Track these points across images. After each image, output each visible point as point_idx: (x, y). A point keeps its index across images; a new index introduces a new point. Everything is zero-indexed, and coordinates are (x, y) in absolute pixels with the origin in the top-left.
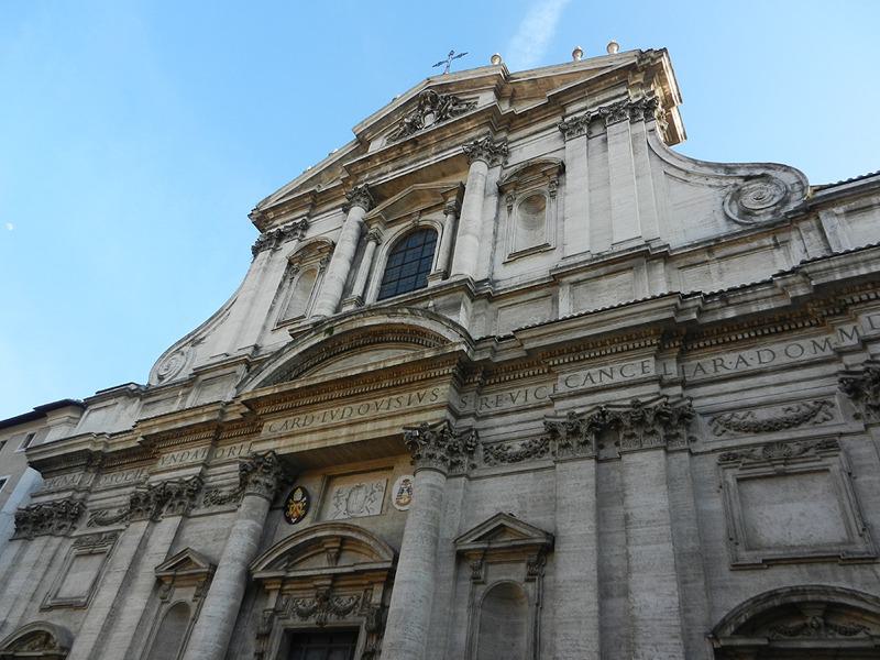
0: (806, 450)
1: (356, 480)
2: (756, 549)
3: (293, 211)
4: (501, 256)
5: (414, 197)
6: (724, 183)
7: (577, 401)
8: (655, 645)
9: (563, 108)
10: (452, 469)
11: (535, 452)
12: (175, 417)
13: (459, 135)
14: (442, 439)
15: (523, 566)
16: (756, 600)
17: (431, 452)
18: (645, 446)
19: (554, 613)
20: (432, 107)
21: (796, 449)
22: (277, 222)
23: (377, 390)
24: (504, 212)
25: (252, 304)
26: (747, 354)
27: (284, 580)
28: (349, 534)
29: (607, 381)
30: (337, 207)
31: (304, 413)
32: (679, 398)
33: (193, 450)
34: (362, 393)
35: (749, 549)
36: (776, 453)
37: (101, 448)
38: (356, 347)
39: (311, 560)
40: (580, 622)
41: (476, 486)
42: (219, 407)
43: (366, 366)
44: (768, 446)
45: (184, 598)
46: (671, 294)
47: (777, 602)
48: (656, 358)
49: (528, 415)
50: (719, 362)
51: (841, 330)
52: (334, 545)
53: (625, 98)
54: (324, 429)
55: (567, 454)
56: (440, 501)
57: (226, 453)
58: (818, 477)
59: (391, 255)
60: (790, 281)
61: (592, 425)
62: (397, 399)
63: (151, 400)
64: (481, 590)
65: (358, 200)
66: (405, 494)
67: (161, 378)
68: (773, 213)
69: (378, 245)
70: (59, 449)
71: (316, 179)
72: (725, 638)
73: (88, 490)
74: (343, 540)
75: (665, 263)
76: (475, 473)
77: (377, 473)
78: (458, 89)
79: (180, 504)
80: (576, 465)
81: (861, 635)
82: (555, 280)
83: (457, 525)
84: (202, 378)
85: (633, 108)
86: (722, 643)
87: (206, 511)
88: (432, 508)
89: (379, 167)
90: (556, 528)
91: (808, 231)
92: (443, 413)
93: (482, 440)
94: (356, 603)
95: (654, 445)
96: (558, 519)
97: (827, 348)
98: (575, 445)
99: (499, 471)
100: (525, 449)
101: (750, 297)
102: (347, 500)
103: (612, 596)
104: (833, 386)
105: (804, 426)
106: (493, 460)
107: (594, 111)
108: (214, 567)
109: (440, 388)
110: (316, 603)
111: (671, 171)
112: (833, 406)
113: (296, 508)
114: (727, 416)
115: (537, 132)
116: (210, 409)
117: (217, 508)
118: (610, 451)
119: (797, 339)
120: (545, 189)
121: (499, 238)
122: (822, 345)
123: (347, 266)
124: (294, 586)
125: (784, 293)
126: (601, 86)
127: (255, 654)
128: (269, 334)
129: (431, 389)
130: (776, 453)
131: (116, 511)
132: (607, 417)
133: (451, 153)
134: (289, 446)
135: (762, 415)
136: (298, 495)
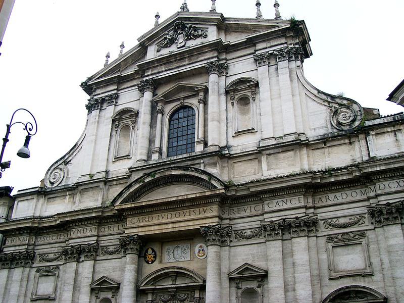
0: (355, 236)
2: (338, 272)
3: (107, 85)
4: (231, 133)
5: (182, 89)
7: (273, 215)
9: (255, 45)
10: (222, 244)
11: (256, 235)
14: (218, 232)
17: (214, 238)
18: (300, 235)
19: (269, 298)
21: (352, 235)
22: (98, 91)
24: (230, 105)
25: (95, 143)
26: (338, 194)
28: (181, 271)
29: (285, 206)
30: (133, 86)
32: (313, 215)
35: (335, 272)
36: (346, 237)
37: (36, 225)
39: (163, 280)
41: (233, 249)
42: (102, 210)
44: (343, 234)
47: (342, 291)
48: (304, 196)
49: (253, 219)
50: (327, 197)
51: (370, 188)
56: (219, 257)
59: (170, 120)
60: (354, 169)
63: (51, 196)
64: (240, 291)
66: (201, 252)
67: (52, 183)
68: (350, 125)
69: (163, 115)
70: (14, 225)
71: (118, 67)
75: (307, 148)
76: (232, 244)
79: (92, 255)
82: (259, 153)
83: (228, 266)
84: (80, 188)
85: (288, 53)
88: (217, 261)
89: (157, 66)
90: (268, 267)
92: (216, 220)
93: (233, 229)
96: (269, 264)
97: (365, 194)
98: (273, 234)
101: (340, 174)
107: (271, 50)
109: (213, 207)
111: (308, 93)
112: (365, 218)
113: (150, 257)
114: (330, 221)
115: (241, 57)
116: (96, 210)
117: (110, 257)
118: (287, 236)
119: (355, 189)
120: (249, 94)
121: (228, 121)
123: (147, 128)
125: (351, 173)
126: (273, 36)
129: (209, 207)
130: (346, 237)
133: (198, 65)
136: (150, 251)
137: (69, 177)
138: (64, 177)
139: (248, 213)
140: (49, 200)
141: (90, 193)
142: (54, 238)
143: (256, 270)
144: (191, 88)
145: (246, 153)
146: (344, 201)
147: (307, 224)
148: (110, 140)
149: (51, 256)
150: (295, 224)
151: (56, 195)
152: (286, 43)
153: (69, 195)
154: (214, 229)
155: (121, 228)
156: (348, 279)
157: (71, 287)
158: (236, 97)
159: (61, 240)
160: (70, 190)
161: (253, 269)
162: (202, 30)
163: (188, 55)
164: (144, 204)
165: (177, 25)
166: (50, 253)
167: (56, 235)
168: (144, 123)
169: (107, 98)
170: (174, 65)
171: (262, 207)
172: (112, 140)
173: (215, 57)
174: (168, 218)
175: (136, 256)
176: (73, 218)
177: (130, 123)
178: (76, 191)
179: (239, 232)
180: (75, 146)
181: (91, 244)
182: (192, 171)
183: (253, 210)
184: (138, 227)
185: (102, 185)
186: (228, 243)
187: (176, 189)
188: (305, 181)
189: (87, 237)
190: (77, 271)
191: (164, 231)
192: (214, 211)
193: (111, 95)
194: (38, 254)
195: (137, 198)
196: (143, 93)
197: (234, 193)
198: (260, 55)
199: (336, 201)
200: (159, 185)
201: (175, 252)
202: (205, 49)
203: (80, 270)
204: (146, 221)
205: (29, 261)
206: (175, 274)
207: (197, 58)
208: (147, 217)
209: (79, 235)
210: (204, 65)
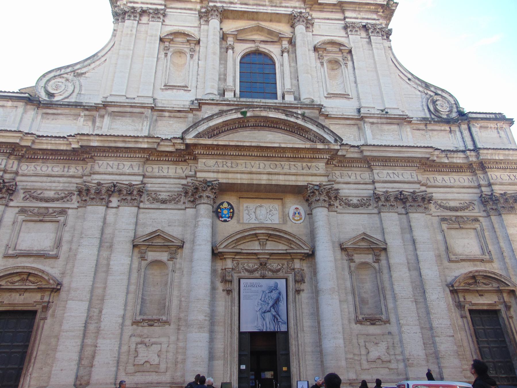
1: (258, 202)
5: (260, 29)
6: (426, 91)
7: (386, 185)
8: (433, 289)
9: (343, 12)
11: (365, 205)
12: (116, 139)
15: (371, 256)
16: (466, 274)
17: (324, 198)
23: (283, 157)
26: (446, 178)
27: (238, 253)
29: (397, 179)
33: (127, 164)
34: (273, 157)
35: (453, 255)
36: (460, 220)
37: (29, 144)
38: (258, 126)
40: (403, 280)
42: (159, 141)
43: (280, 143)
44: (457, 217)
45: (159, 258)
46: (431, 147)
52: (264, 238)
53: (378, 22)
54: (251, 173)
55: (383, 209)
57: (156, 170)
58: (472, 230)
59: (240, 63)
61: (396, 198)
62: (294, 165)
65: (217, 15)
66: (297, 215)
68: (447, 115)
72: (457, 287)
73: (17, 173)
74: (270, 235)
77: (270, 200)
80: (390, 214)
81: (490, 285)
84: (110, 109)
85: (381, 29)
86: (455, 288)
87: (153, 206)
91: (465, 130)
94: (282, 267)
95: (421, 211)
97: (473, 182)
99: (349, 212)
100: (359, 203)
102: (255, 212)
103: (411, 270)
104: (476, 197)
105: (466, 211)
106: (344, 206)
107: (364, 22)
108: (184, 243)
110: (256, 266)
111: (401, 75)
112: (475, 205)
115: (328, 19)
116: (150, 140)
117: (163, 206)
120: (340, 59)
122: (471, 180)
124: (242, 257)
126: (365, 8)
127: (223, 290)
128: (160, 92)
129: (314, 164)
131: (53, 192)
132: (402, 196)
133: (282, 11)
134: (226, 178)
135: (452, 204)
136: (225, 205)
137: (83, 92)
138: (73, 91)
139: (353, 179)
140: (45, 116)
141: (128, 120)
142: (56, 169)
143: (375, 242)
144: (270, 32)
145: (346, 117)
146: (452, 184)
147: (423, 199)
148: (157, 61)
149: (51, 194)
150: (413, 198)
151: (59, 111)
152: (378, 20)
153: (85, 115)
154: (325, 189)
155: (179, 171)
156: (469, 263)
157: (96, 242)
158: (326, 58)
159: (71, 174)
160: (87, 110)
161: (371, 240)
166: (46, 190)
167: (61, 166)
168: (214, 54)
169: (151, 11)
171: (368, 176)
172: (159, 63)
173: (303, 8)
174: (259, 168)
175: (210, 207)
176: (106, 145)
177: (187, 51)
178: (103, 112)
179: (344, 198)
180: (94, 56)
181: (134, 185)
182: (297, 118)
183: (358, 177)
184: (218, 172)
186: (334, 209)
187: (269, 136)
188: (424, 156)
189: (125, 174)
190: (105, 218)
192: (321, 170)
193: (157, 9)
194: (22, 189)
195: (214, 135)
196: (207, 21)
197: (344, 153)
198: (352, 23)
199: (444, 183)
200: (246, 127)
201: (258, 212)
203: (110, 218)
204: (227, 164)
205: (5, 196)
206: (267, 238)
208: (229, 162)
209: (110, 170)
210: (289, 13)
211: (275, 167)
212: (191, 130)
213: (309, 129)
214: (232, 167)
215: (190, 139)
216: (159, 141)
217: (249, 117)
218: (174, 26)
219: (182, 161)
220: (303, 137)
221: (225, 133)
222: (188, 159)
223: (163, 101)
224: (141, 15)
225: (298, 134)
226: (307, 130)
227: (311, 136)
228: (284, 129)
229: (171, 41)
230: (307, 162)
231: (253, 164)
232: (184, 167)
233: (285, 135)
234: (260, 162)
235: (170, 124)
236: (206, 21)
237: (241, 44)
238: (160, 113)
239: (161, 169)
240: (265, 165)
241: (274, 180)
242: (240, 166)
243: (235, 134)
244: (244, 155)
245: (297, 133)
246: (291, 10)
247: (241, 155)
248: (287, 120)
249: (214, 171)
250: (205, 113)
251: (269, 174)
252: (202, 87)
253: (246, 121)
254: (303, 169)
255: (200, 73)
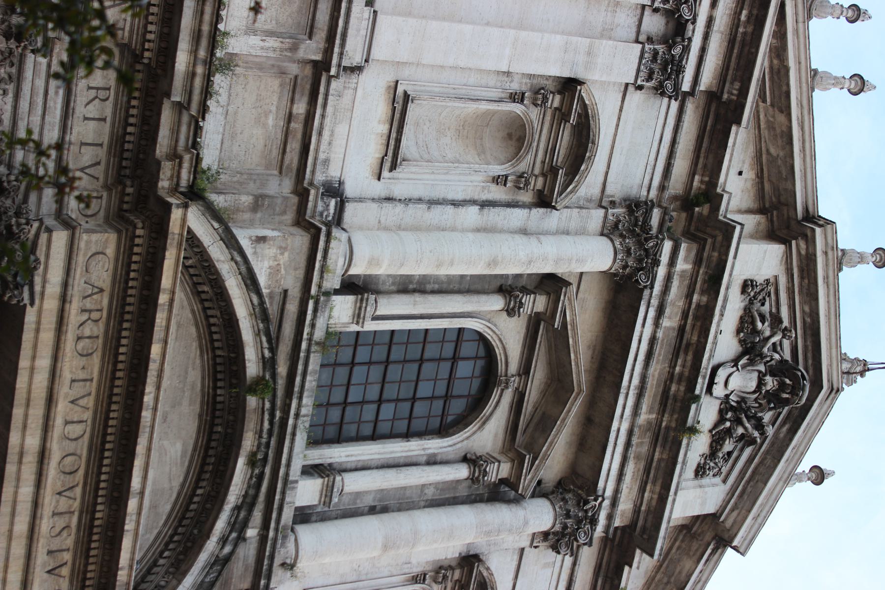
3: (731, 42)
13: (647, 470)
20: (767, 391)
31: (106, 332)
34: (101, 466)
38: (214, 417)
43: (142, 493)
54: (50, 401)
65: (625, 267)
78: (772, 444)
89: (689, 296)
116: (198, 82)
133: (611, 461)
134: (39, 323)
155: (88, 156)
162: (729, 454)
163: (668, 428)
164: (155, 350)
165: (796, 389)
169: (677, 51)
170: (657, 369)
174: (67, 423)
177: (523, 166)
182: (223, 541)
184: (64, 299)
185: (312, 50)
187: (179, 446)
191: (18, 412)
193: (680, 70)
195: (195, 284)
200: (215, 380)
202: (652, 492)
207: (637, 458)
208: (98, 330)
210: (601, 484)
211: (67, 470)
212: (216, 225)
213: (184, 574)
214: (79, 338)
215: (184, 220)
216: (194, 112)
217: (245, 400)
218: (619, 119)
219: (121, 168)
220: (162, 552)
221: (200, 316)
222: (123, 194)
223: (351, 91)
224: (669, 14)
225: (172, 536)
226: (183, 567)
227: (160, 577)
228: (194, 494)
229: (563, 114)
230: (74, 564)
231: (82, 402)
232: (99, 171)
233: (174, 496)
234: (89, 422)
235: (266, 116)
236: (616, 225)
237: (524, 331)
238: (308, 87)
239: (102, 94)
240: (76, 439)
241: (19, 470)
242: (83, 361)
243: (195, 344)
244: (114, 378)
245: (175, 533)
246: (609, 493)
247: (115, 370)
248: (220, 510)
249: (70, 288)
250: (280, 248)
251: (43, 455)
252: (383, 221)
253: (234, 381)
254: (50, 552)
255: (437, 210)
